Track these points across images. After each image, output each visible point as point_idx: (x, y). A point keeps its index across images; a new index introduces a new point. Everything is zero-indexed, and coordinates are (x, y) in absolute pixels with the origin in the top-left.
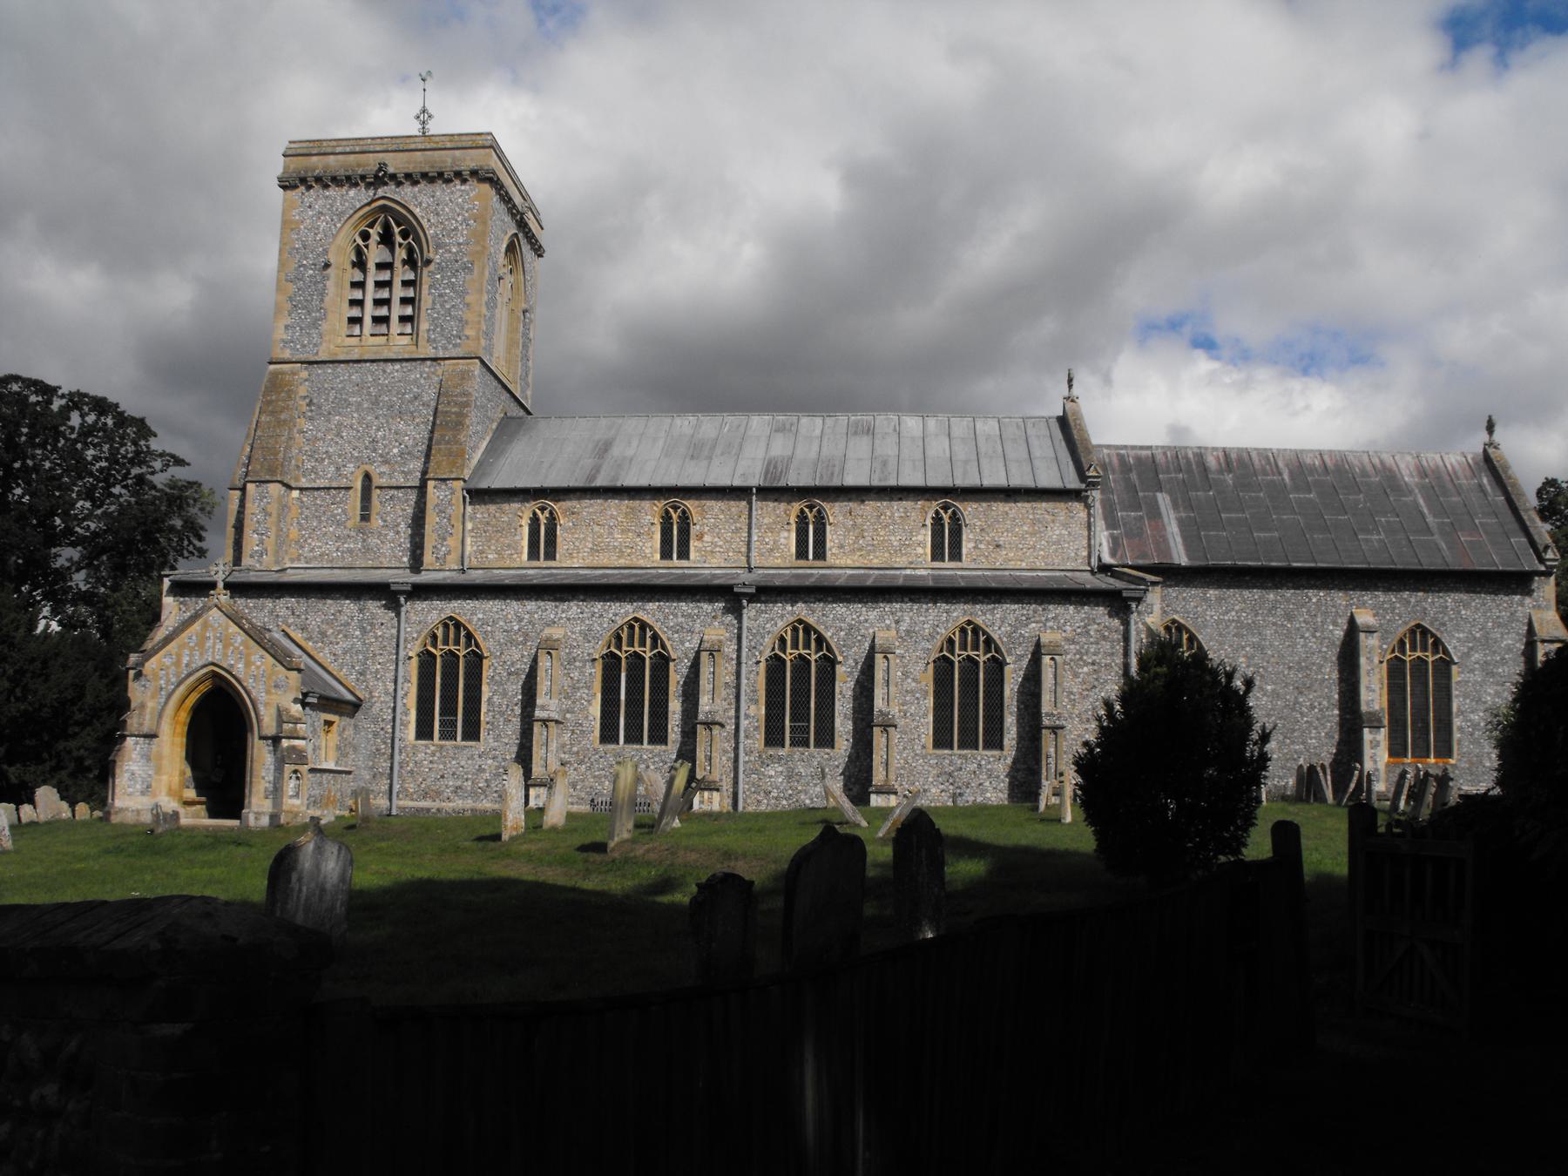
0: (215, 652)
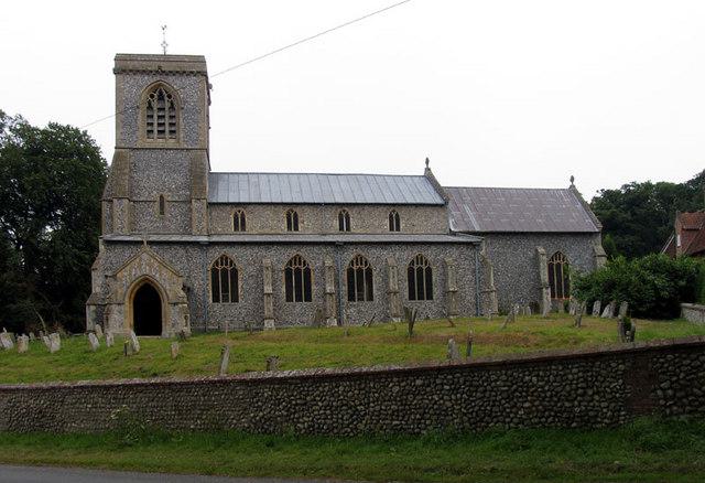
0: (146, 270)
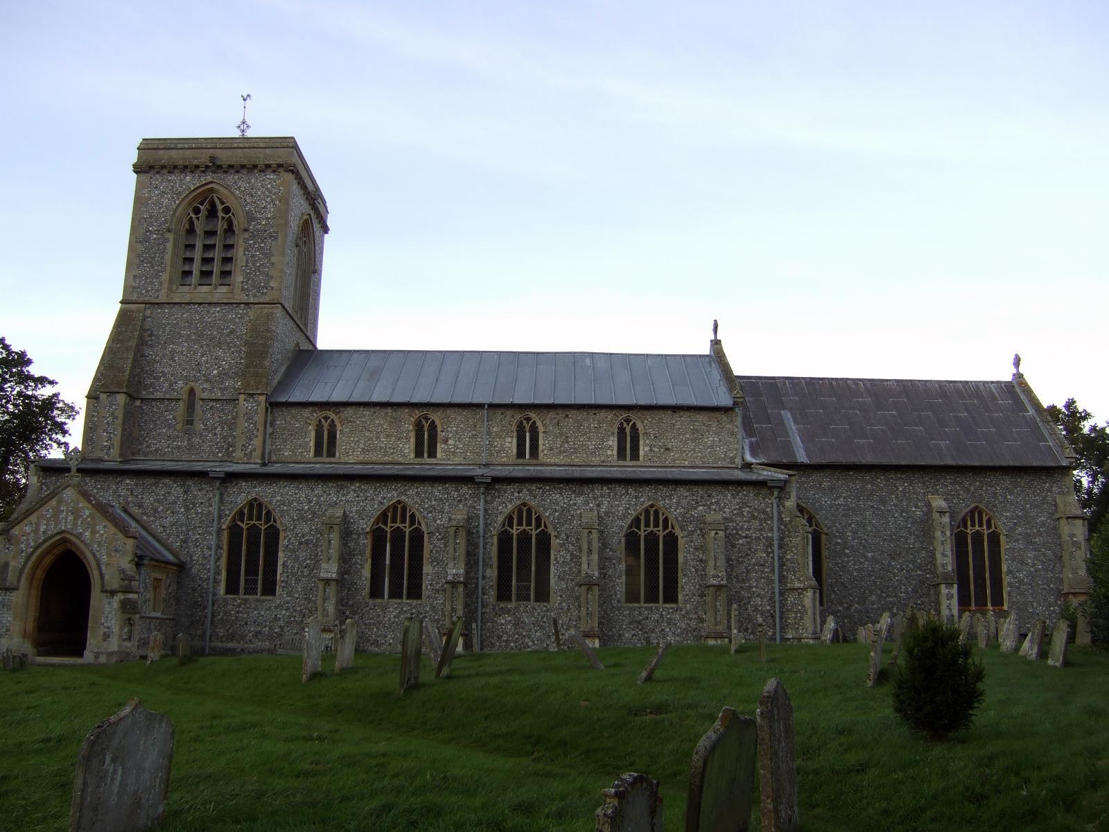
0: (67, 522)
